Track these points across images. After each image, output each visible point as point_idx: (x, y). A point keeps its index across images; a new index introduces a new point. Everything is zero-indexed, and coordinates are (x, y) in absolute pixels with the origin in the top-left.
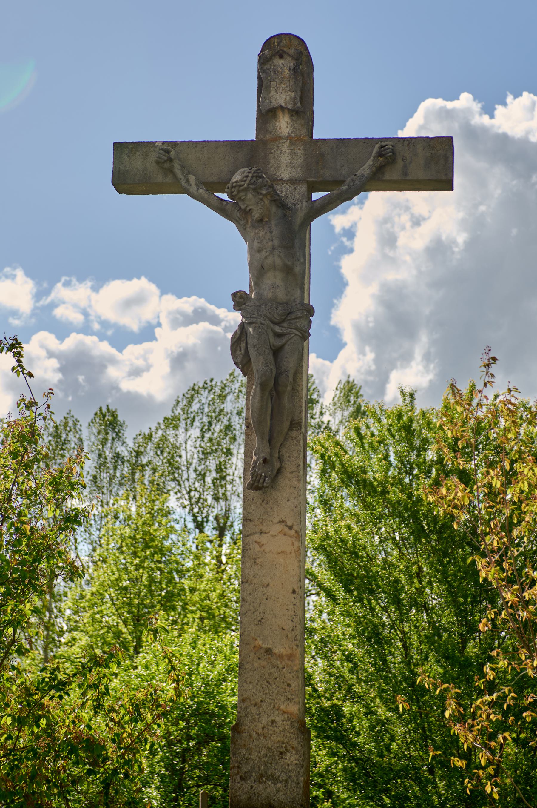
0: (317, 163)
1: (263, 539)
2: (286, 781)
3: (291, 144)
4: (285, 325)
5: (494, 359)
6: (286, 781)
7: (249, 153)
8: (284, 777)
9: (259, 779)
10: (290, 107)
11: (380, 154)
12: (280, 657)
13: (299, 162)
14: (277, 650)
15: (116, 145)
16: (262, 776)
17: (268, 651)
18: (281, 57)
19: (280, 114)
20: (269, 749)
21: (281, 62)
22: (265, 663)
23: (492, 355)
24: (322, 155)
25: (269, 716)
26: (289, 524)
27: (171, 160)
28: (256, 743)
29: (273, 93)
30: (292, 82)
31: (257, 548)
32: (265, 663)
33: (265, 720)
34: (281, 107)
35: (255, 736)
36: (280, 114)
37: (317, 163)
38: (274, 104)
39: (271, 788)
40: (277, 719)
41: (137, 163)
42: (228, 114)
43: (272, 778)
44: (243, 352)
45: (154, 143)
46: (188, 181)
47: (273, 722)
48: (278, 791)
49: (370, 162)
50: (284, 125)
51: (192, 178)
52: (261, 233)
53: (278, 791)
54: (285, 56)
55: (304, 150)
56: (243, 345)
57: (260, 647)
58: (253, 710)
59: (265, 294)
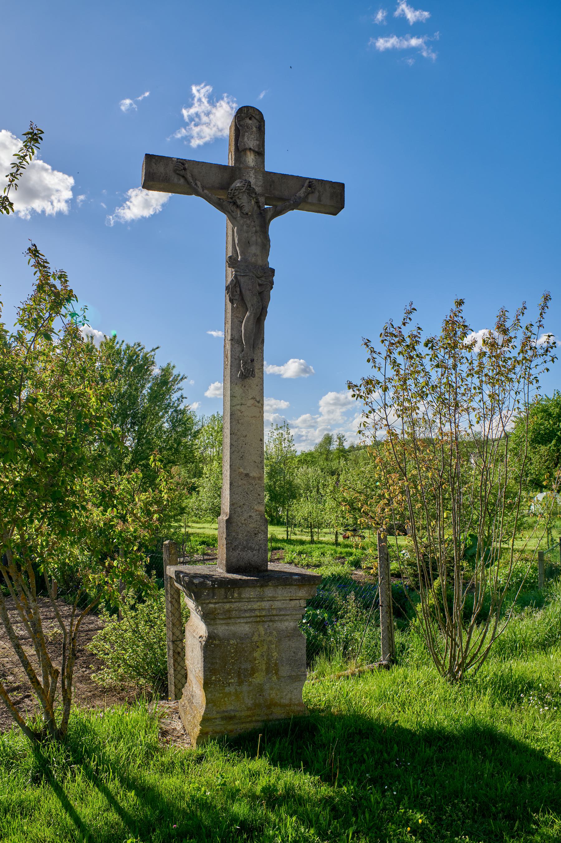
0: (271, 186)
1: (243, 408)
2: (259, 550)
3: (256, 172)
4: (263, 279)
5: (414, 309)
6: (259, 550)
7: (231, 173)
8: (257, 547)
9: (243, 550)
10: (256, 150)
11: (310, 186)
12: (254, 478)
13: (260, 183)
14: (251, 475)
15: (147, 156)
16: (245, 547)
17: (247, 475)
18: (250, 119)
19: (248, 153)
20: (248, 532)
21: (250, 122)
22: (245, 482)
23: (413, 307)
24: (273, 182)
25: (248, 513)
26: (258, 400)
27: (185, 169)
28: (241, 528)
29: (246, 139)
30: (258, 135)
31: (240, 414)
32: (245, 482)
33: (246, 515)
34: (250, 149)
35: (240, 525)
36: (248, 153)
37: (271, 186)
38: (247, 146)
39: (250, 554)
40: (253, 515)
41: (161, 169)
42: (282, 158)
43: (252, 549)
44: (238, 293)
45: (171, 158)
46: (196, 184)
47: (250, 516)
48: (254, 556)
49: (303, 190)
50: (250, 159)
51: (199, 184)
52: (248, 222)
53: (254, 556)
54: (253, 119)
55: (263, 177)
56: (238, 289)
57: (242, 473)
58: (239, 509)
59: (249, 259)
